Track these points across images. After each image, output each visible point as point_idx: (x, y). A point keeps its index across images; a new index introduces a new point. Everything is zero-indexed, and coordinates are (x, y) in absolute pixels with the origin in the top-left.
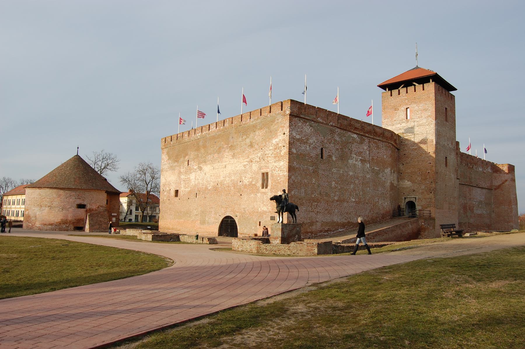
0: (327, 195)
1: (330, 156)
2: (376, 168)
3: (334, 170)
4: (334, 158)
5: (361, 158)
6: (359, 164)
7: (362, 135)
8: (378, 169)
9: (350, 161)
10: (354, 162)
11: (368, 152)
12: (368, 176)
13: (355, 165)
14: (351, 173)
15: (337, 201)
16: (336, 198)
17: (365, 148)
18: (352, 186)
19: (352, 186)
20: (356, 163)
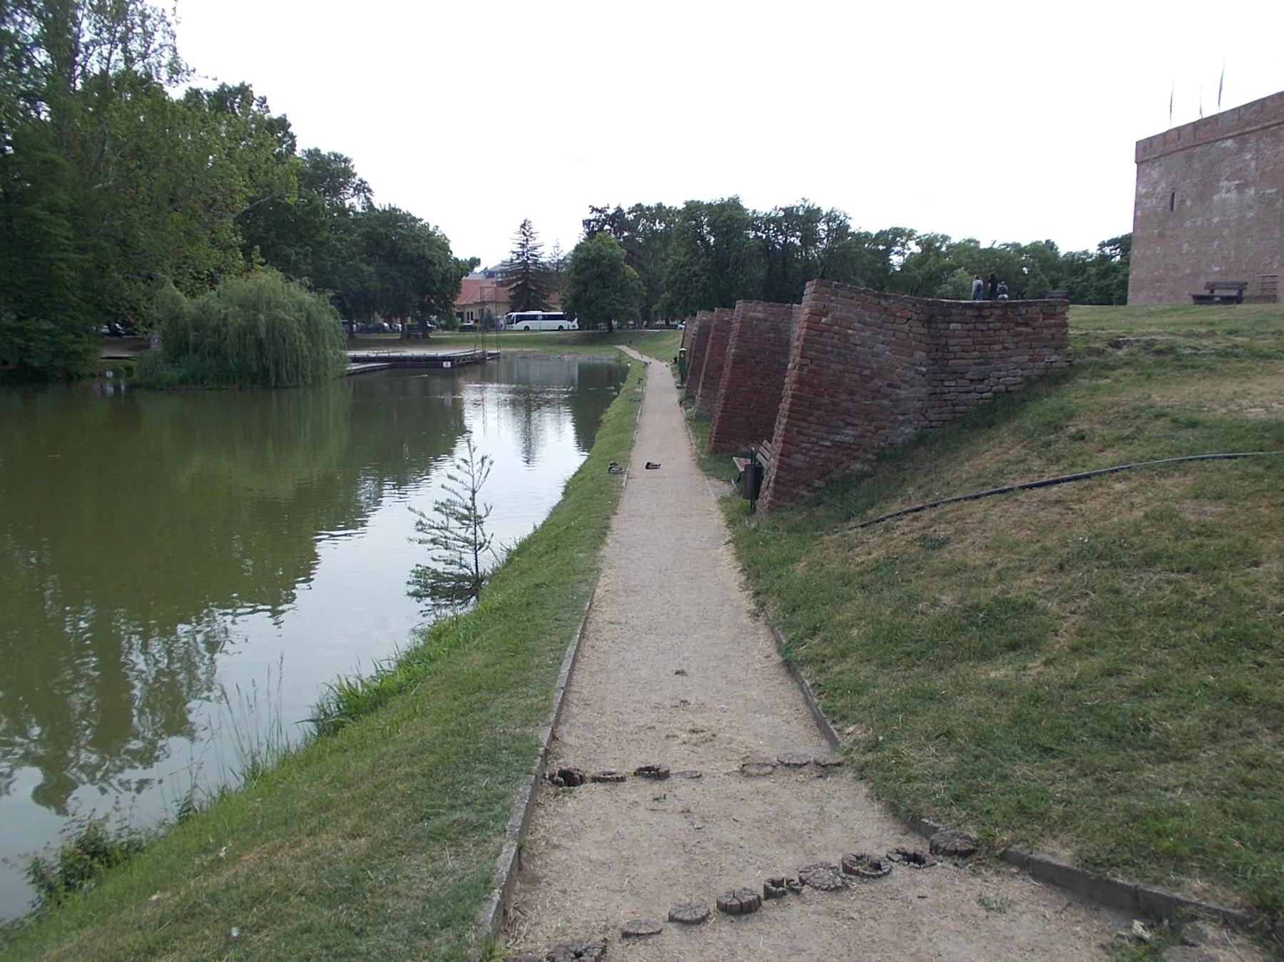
0: (1175, 269)
1: (1183, 202)
2: (1268, 191)
3: (1188, 224)
4: (1189, 203)
5: (1237, 182)
6: (1233, 196)
7: (1240, 135)
8: (1274, 190)
9: (1216, 198)
10: (1224, 196)
11: (1253, 164)
12: (1250, 214)
13: (1224, 200)
14: (1216, 220)
15: (1189, 275)
16: (1188, 271)
17: (1248, 156)
18: (1216, 244)
19: (1216, 244)
20: (1228, 196)
